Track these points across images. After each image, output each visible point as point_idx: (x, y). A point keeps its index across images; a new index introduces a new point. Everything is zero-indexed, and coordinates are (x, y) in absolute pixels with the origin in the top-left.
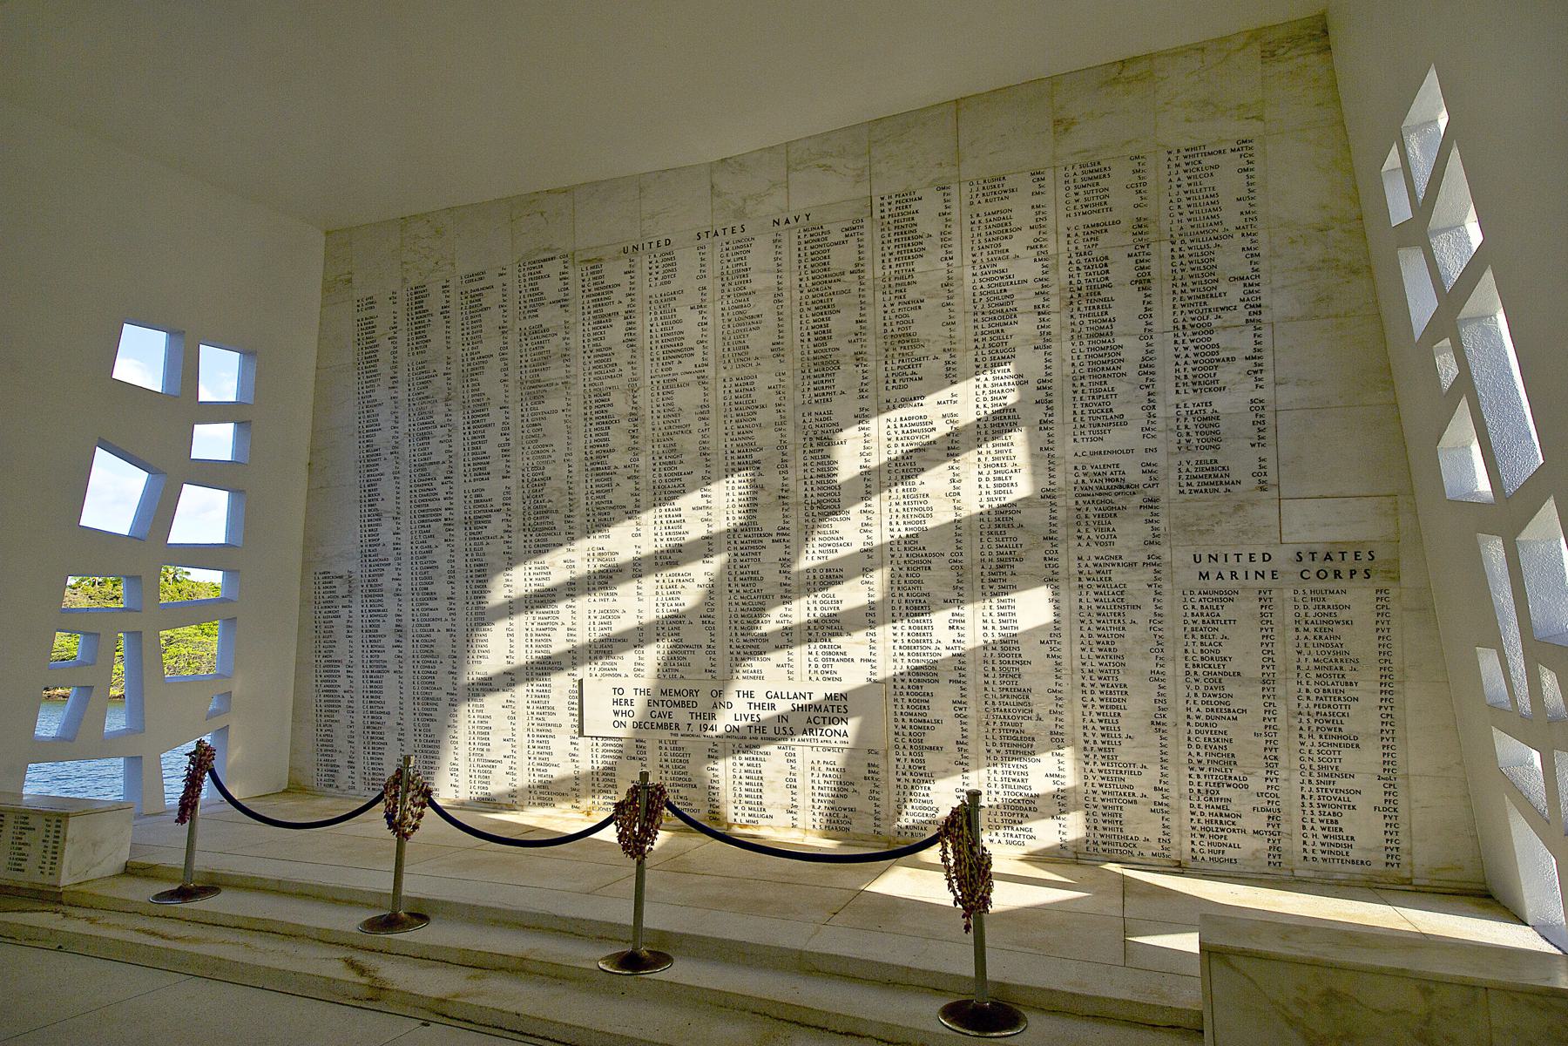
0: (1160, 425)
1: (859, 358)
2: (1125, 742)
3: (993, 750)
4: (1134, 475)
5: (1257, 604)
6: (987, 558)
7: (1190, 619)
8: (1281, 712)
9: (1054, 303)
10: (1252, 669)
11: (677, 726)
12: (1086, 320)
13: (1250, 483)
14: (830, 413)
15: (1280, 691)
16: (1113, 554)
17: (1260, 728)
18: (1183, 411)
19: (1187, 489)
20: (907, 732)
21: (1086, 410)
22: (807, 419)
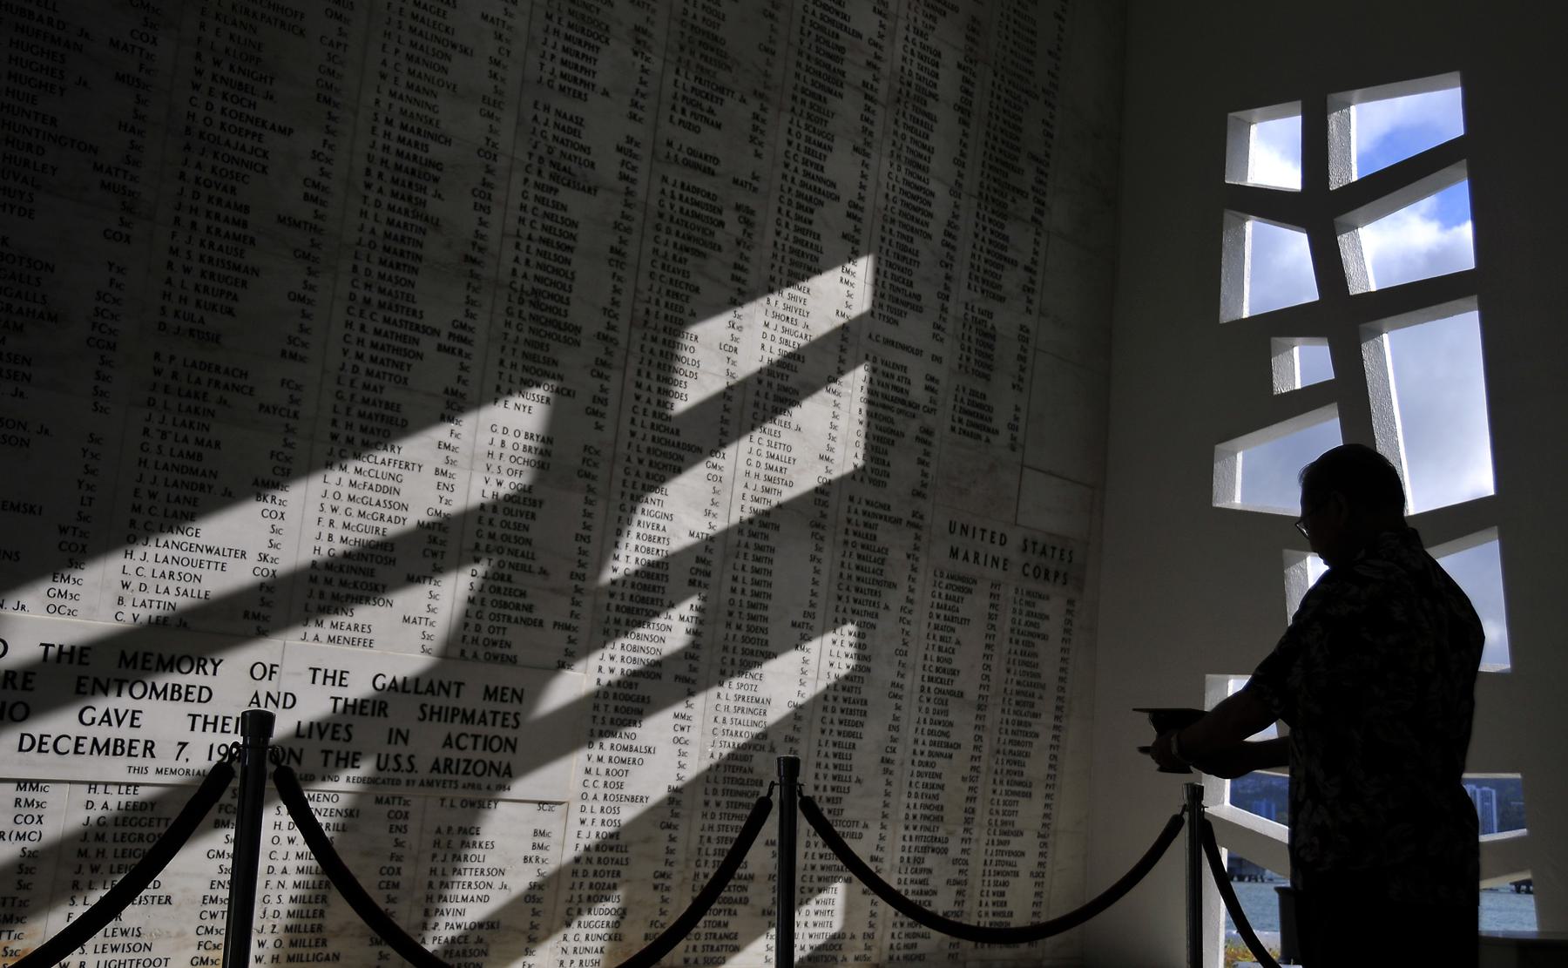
0: (949, 326)
1: (640, 39)
2: (854, 787)
3: (713, 800)
4: (918, 393)
5: (987, 601)
6: (753, 470)
7: (935, 611)
8: (986, 750)
9: (882, 87)
10: (972, 693)
11: (149, 748)
12: (909, 134)
13: (1004, 437)
14: (580, 121)
15: (988, 723)
16: (883, 500)
17: (967, 772)
18: (970, 314)
19: (958, 426)
20: (603, 767)
21: (889, 271)
22: (542, 116)
